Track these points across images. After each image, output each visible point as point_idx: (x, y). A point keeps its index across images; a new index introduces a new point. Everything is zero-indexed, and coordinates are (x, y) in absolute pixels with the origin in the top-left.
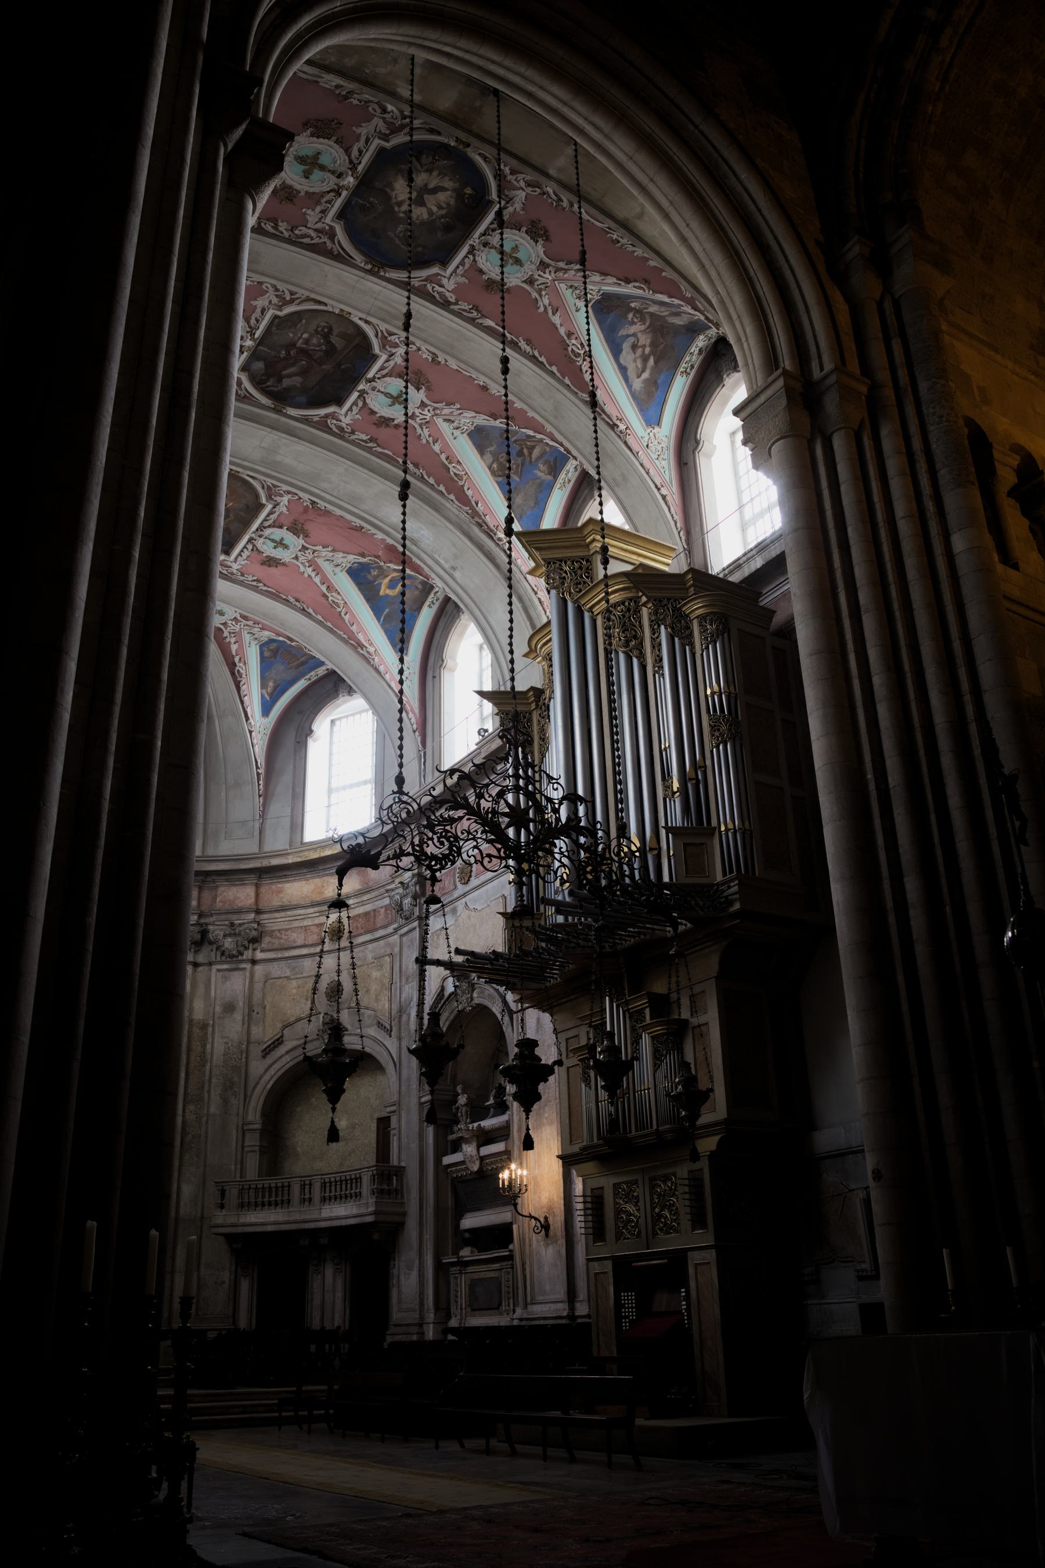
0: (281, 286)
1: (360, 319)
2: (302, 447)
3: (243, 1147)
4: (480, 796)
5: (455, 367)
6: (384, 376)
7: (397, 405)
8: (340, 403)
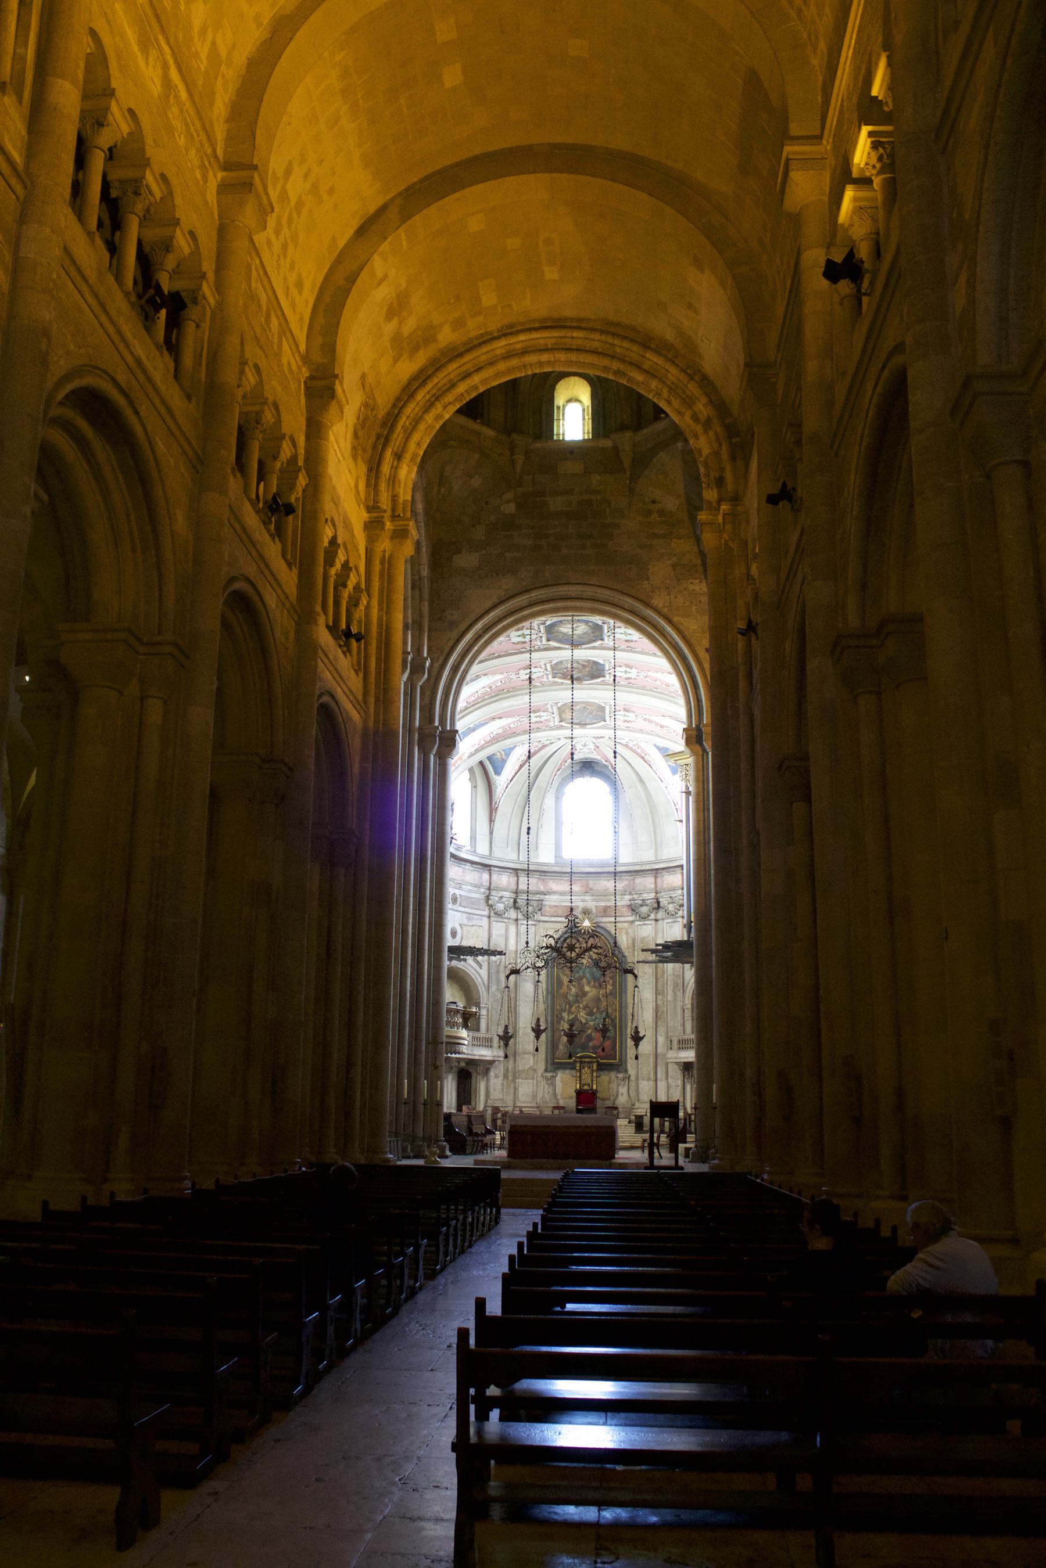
3: (684, 1018)
8: (604, 676)
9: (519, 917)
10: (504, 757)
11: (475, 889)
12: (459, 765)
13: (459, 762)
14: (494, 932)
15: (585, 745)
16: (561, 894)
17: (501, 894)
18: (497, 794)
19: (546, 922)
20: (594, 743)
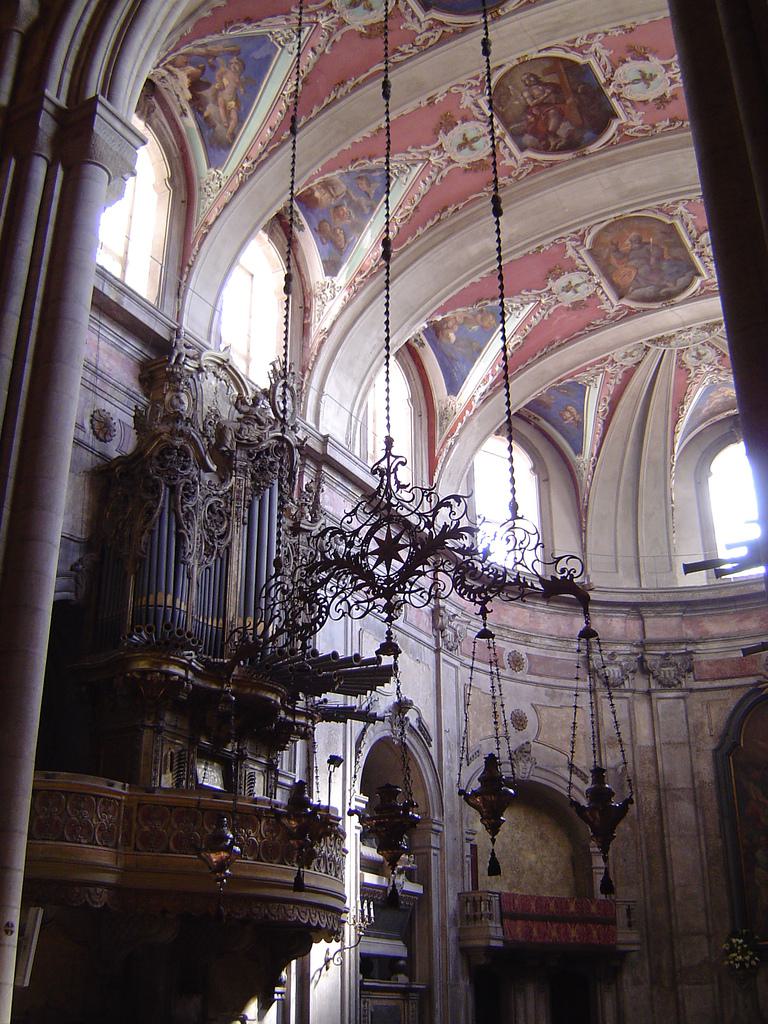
0: (462, 81)
1: (539, 51)
2: (632, 167)
4: (350, 544)
5: (647, 21)
6: (613, 72)
7: (651, 83)
8: (615, 116)
9: (653, 687)
10: (578, 417)
11: (559, 644)
12: (469, 419)
13: (467, 412)
14: (607, 717)
15: (699, 356)
16: (726, 638)
17: (613, 648)
18: (584, 484)
19: (705, 690)
20: (713, 347)
